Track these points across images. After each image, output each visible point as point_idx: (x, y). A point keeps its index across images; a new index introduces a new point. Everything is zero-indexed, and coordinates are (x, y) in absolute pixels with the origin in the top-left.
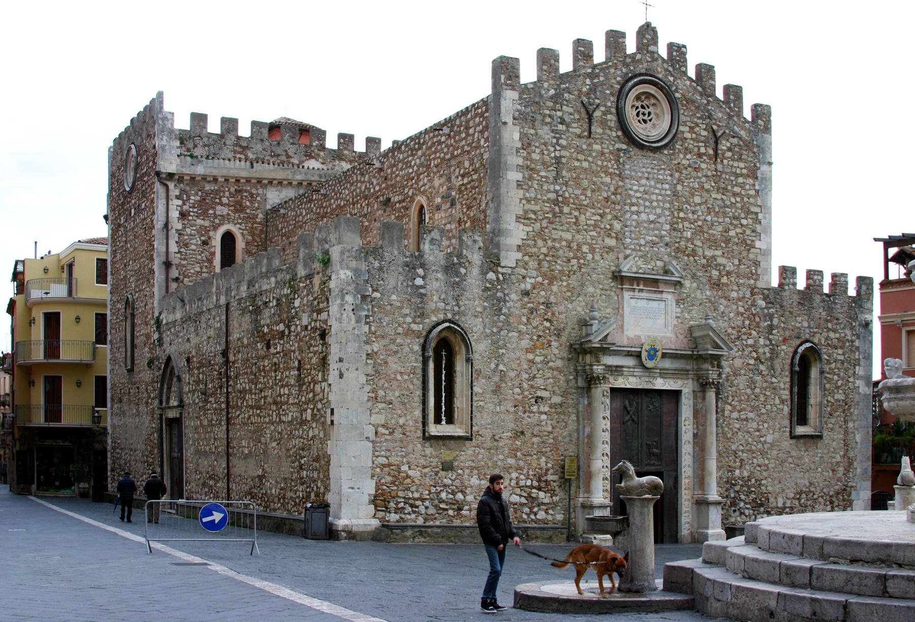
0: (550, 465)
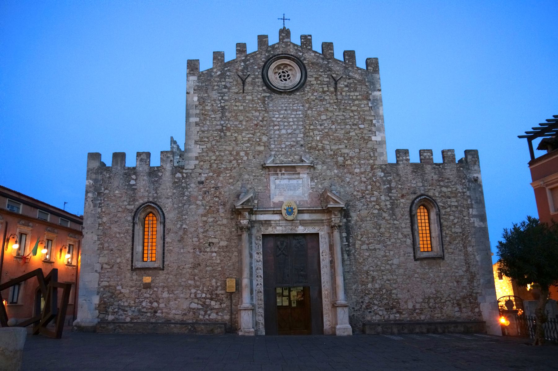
0: (219, 284)
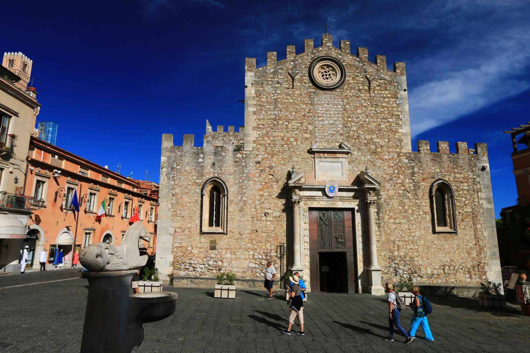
0: (273, 248)
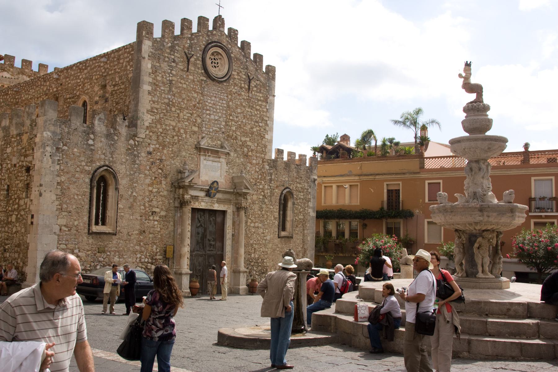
0: (158, 250)
